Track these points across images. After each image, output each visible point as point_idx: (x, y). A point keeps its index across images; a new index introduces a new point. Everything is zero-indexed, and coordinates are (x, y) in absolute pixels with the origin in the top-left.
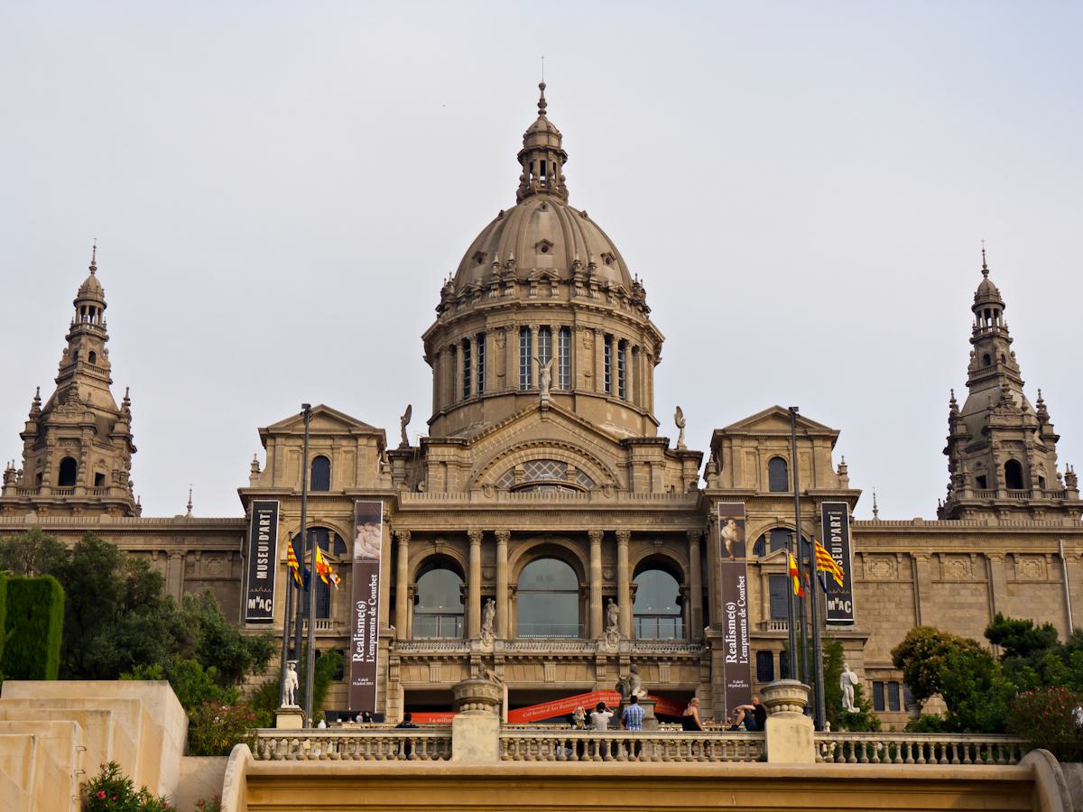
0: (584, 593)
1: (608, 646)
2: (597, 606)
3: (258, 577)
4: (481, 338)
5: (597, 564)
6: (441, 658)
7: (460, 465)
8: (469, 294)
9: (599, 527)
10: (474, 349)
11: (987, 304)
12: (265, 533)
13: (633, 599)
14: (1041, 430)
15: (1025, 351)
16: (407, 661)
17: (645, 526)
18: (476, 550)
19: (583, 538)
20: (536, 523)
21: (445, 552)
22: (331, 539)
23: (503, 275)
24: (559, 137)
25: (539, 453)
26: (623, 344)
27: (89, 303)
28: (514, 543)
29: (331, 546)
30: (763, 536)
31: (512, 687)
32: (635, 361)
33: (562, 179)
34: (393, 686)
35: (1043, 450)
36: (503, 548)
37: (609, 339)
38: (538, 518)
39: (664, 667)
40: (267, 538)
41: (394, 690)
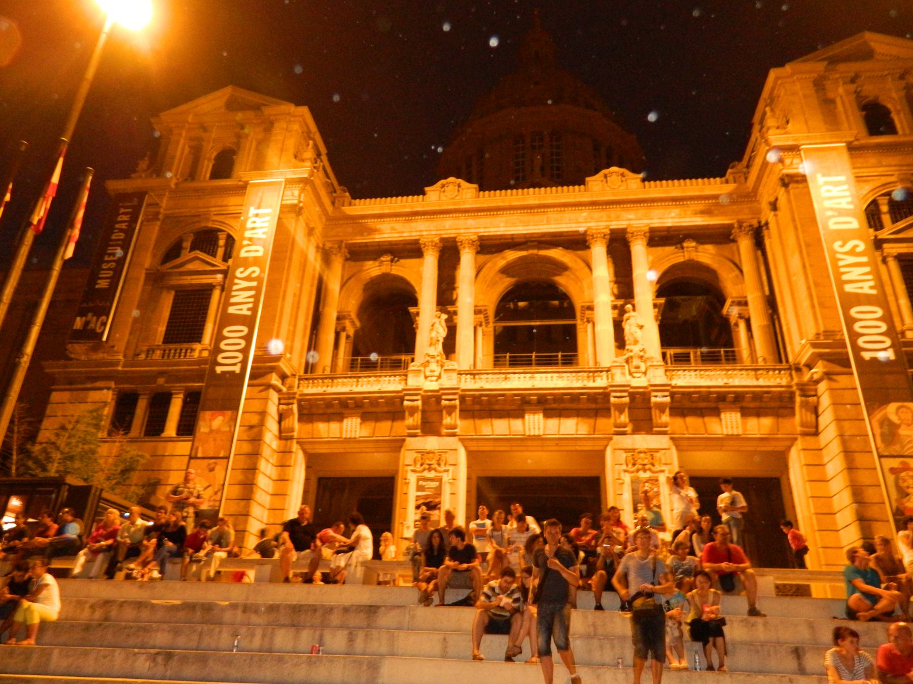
1: (628, 377)
3: (97, 286)
9: (603, 224)
12: (121, 230)
17: (670, 220)
19: (577, 243)
20: (514, 225)
21: (393, 272)
22: (222, 242)
28: (482, 258)
29: (220, 252)
30: (874, 203)
31: (474, 447)
34: (286, 446)
38: (516, 216)
40: (122, 236)
41: (285, 452)
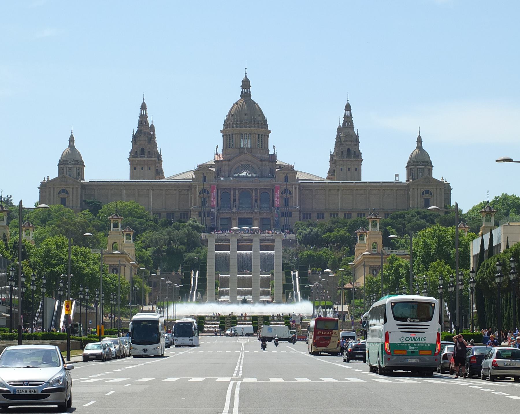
0: (252, 199)
2: (254, 202)
4: (232, 135)
5: (254, 194)
6: (226, 213)
7: (229, 165)
8: (230, 123)
10: (231, 136)
11: (348, 107)
13: (260, 199)
14: (356, 140)
15: (355, 120)
16: (220, 213)
18: (232, 191)
23: (237, 121)
24: (249, 82)
25: (244, 163)
26: (262, 135)
27: (144, 107)
32: (264, 138)
33: (250, 92)
35: (356, 145)
36: (237, 191)
37: (259, 135)
39: (265, 214)
